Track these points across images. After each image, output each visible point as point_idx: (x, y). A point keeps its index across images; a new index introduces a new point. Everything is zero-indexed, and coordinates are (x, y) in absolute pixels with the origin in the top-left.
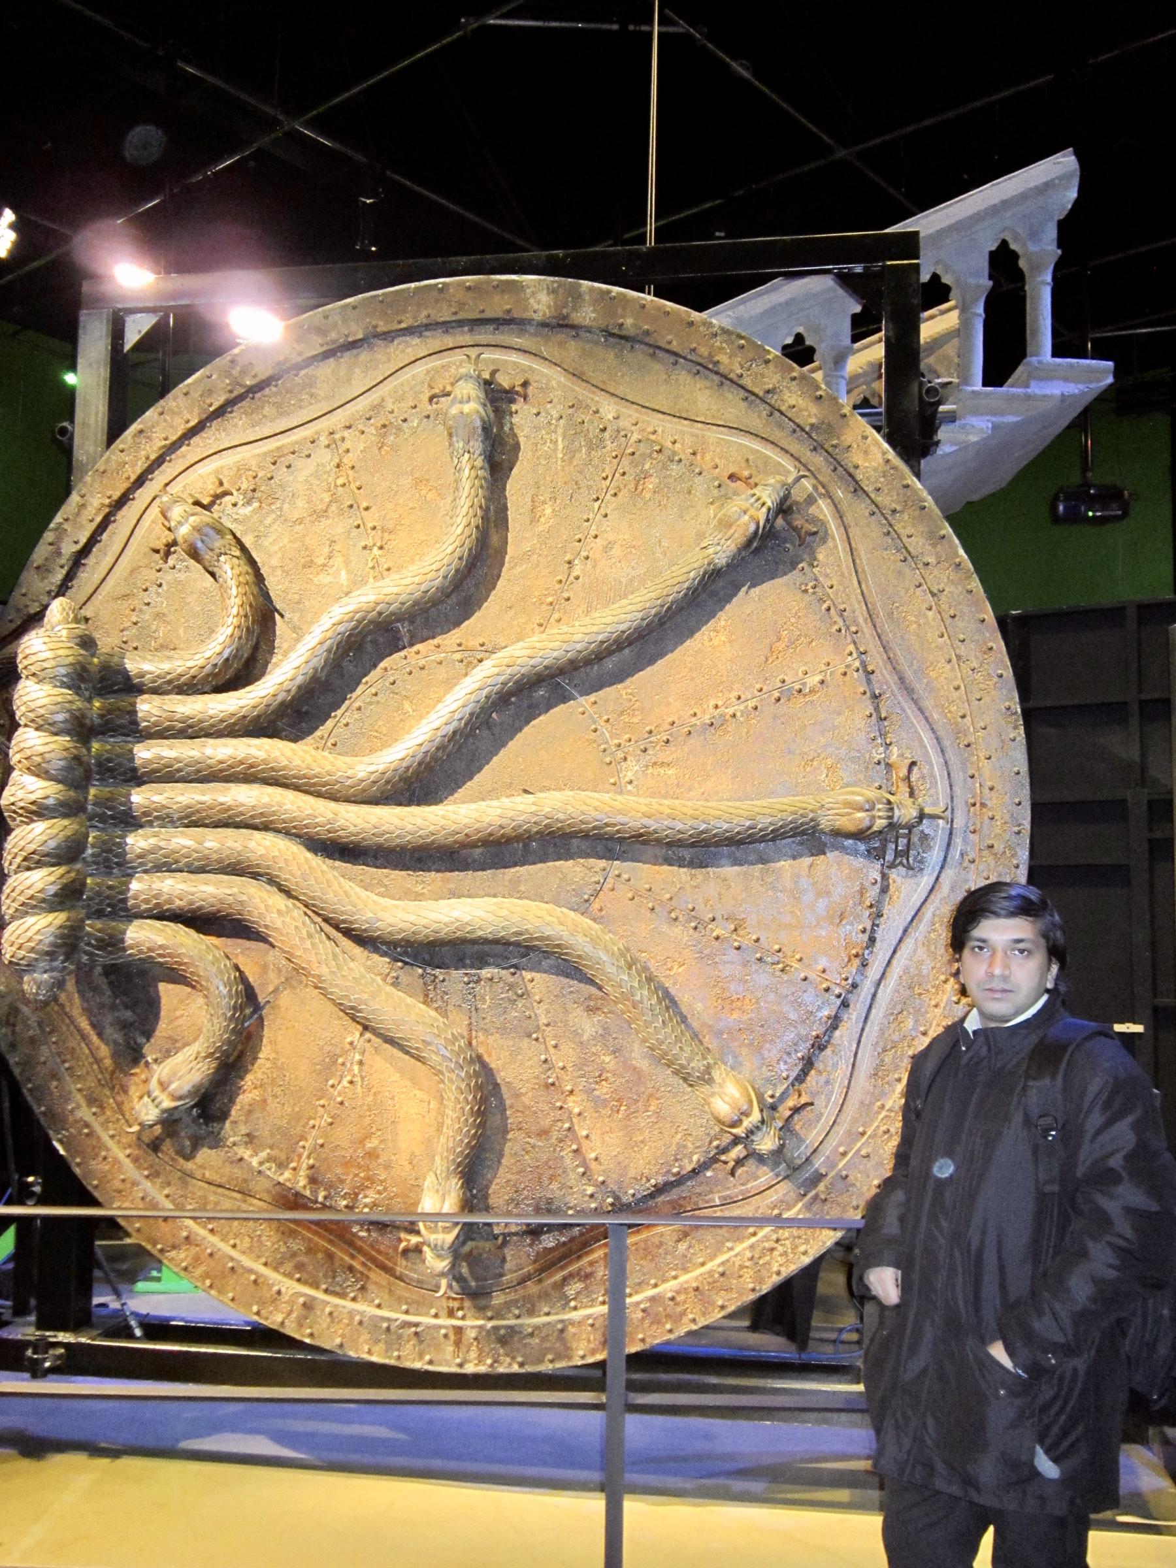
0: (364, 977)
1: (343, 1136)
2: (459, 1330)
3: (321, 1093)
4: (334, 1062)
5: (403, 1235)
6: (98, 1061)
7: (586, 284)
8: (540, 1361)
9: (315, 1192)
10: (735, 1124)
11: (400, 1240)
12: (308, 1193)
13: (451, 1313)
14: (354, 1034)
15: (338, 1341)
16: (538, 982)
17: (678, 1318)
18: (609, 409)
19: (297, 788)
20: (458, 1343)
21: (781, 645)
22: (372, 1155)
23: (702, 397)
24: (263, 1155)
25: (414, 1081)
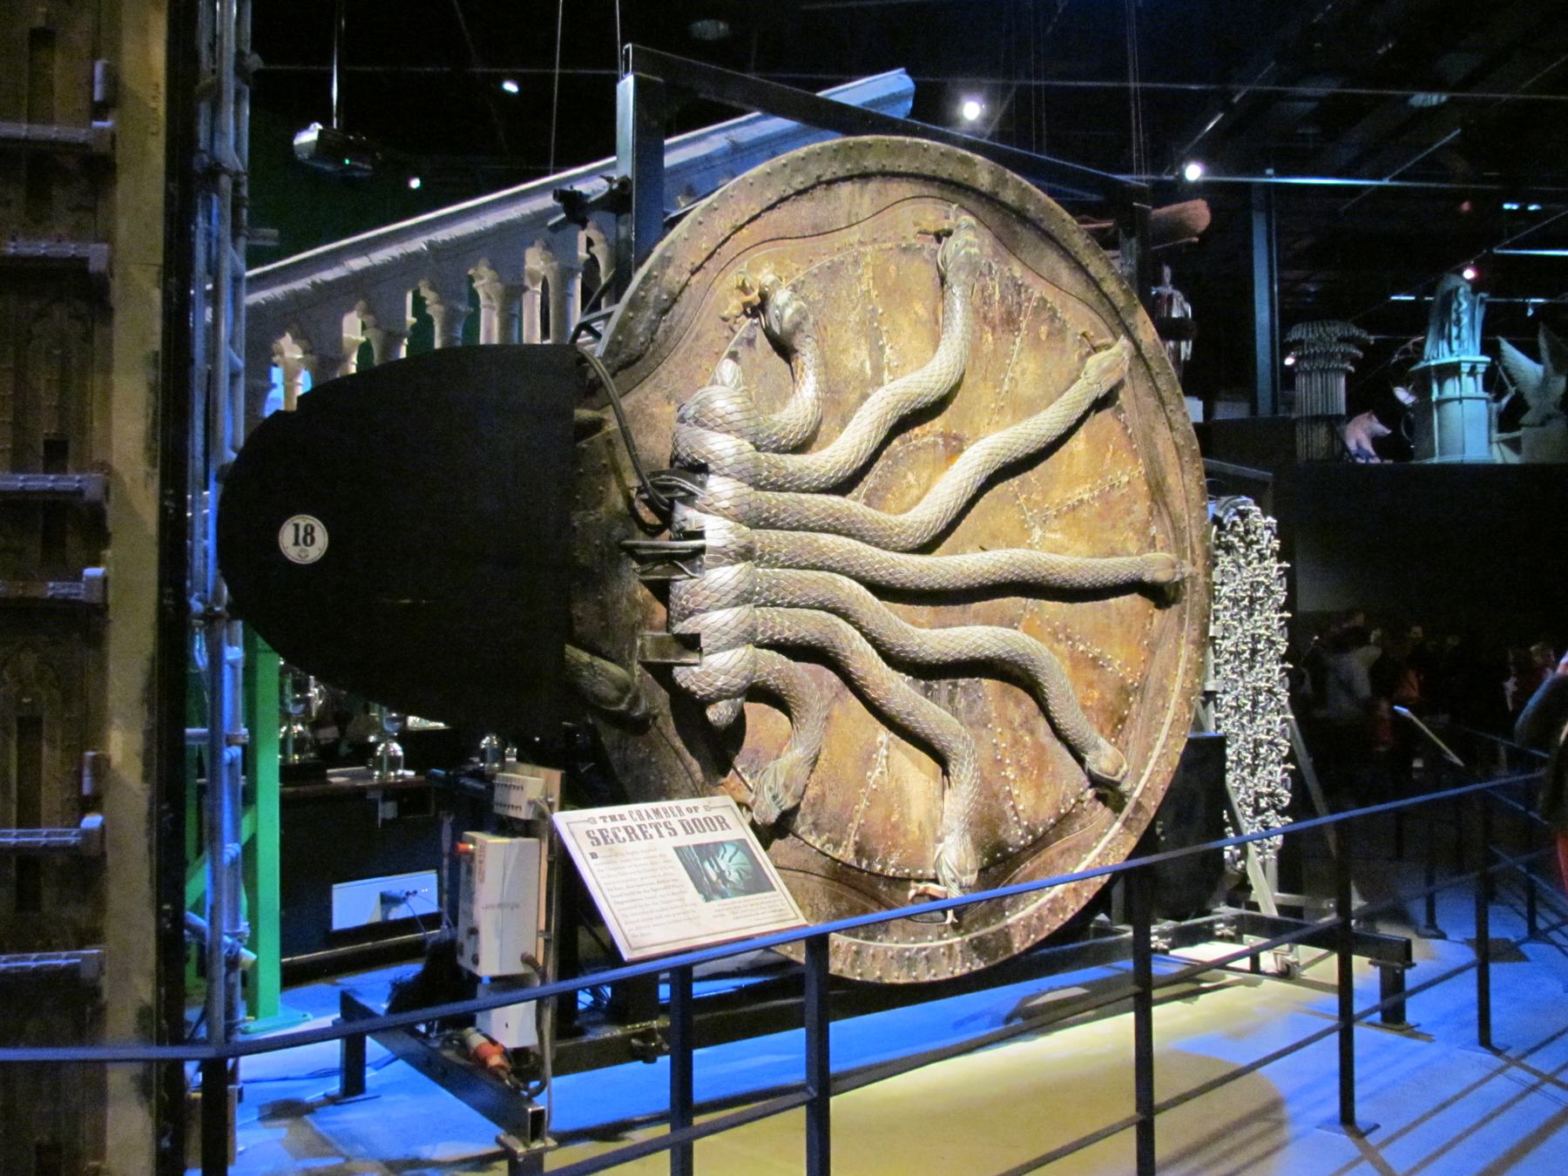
0: (898, 690)
1: (878, 813)
2: (950, 947)
3: (863, 782)
4: (870, 758)
5: (913, 884)
6: (691, 775)
7: (1009, 174)
8: (996, 956)
9: (859, 862)
10: (1117, 773)
11: (908, 889)
12: (855, 864)
13: (940, 937)
14: (884, 735)
15: (878, 973)
16: (988, 685)
17: (1064, 909)
18: (1018, 271)
19: (862, 539)
20: (950, 956)
21: (1109, 455)
22: (895, 827)
23: (1065, 274)
24: (825, 838)
25: (919, 766)
